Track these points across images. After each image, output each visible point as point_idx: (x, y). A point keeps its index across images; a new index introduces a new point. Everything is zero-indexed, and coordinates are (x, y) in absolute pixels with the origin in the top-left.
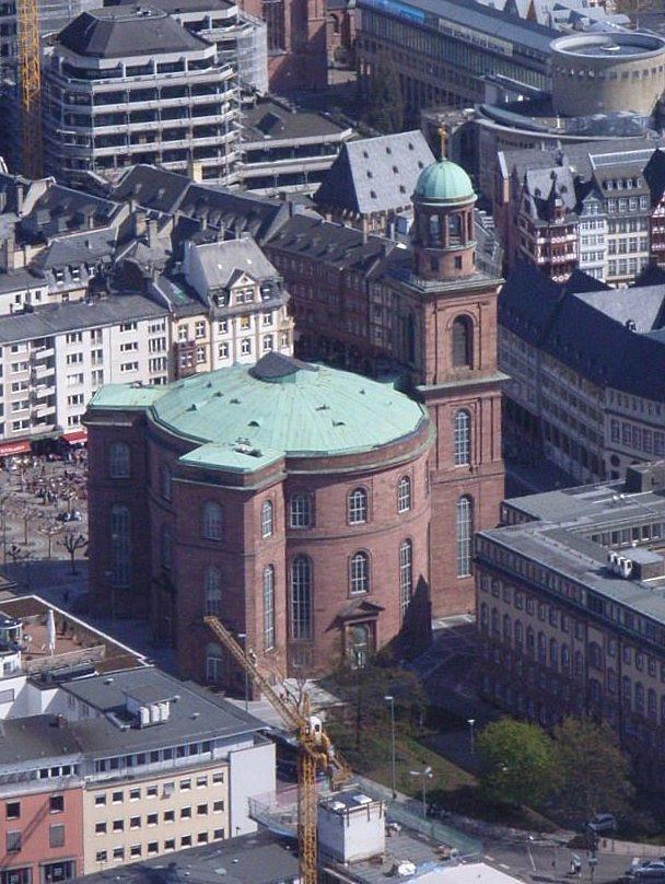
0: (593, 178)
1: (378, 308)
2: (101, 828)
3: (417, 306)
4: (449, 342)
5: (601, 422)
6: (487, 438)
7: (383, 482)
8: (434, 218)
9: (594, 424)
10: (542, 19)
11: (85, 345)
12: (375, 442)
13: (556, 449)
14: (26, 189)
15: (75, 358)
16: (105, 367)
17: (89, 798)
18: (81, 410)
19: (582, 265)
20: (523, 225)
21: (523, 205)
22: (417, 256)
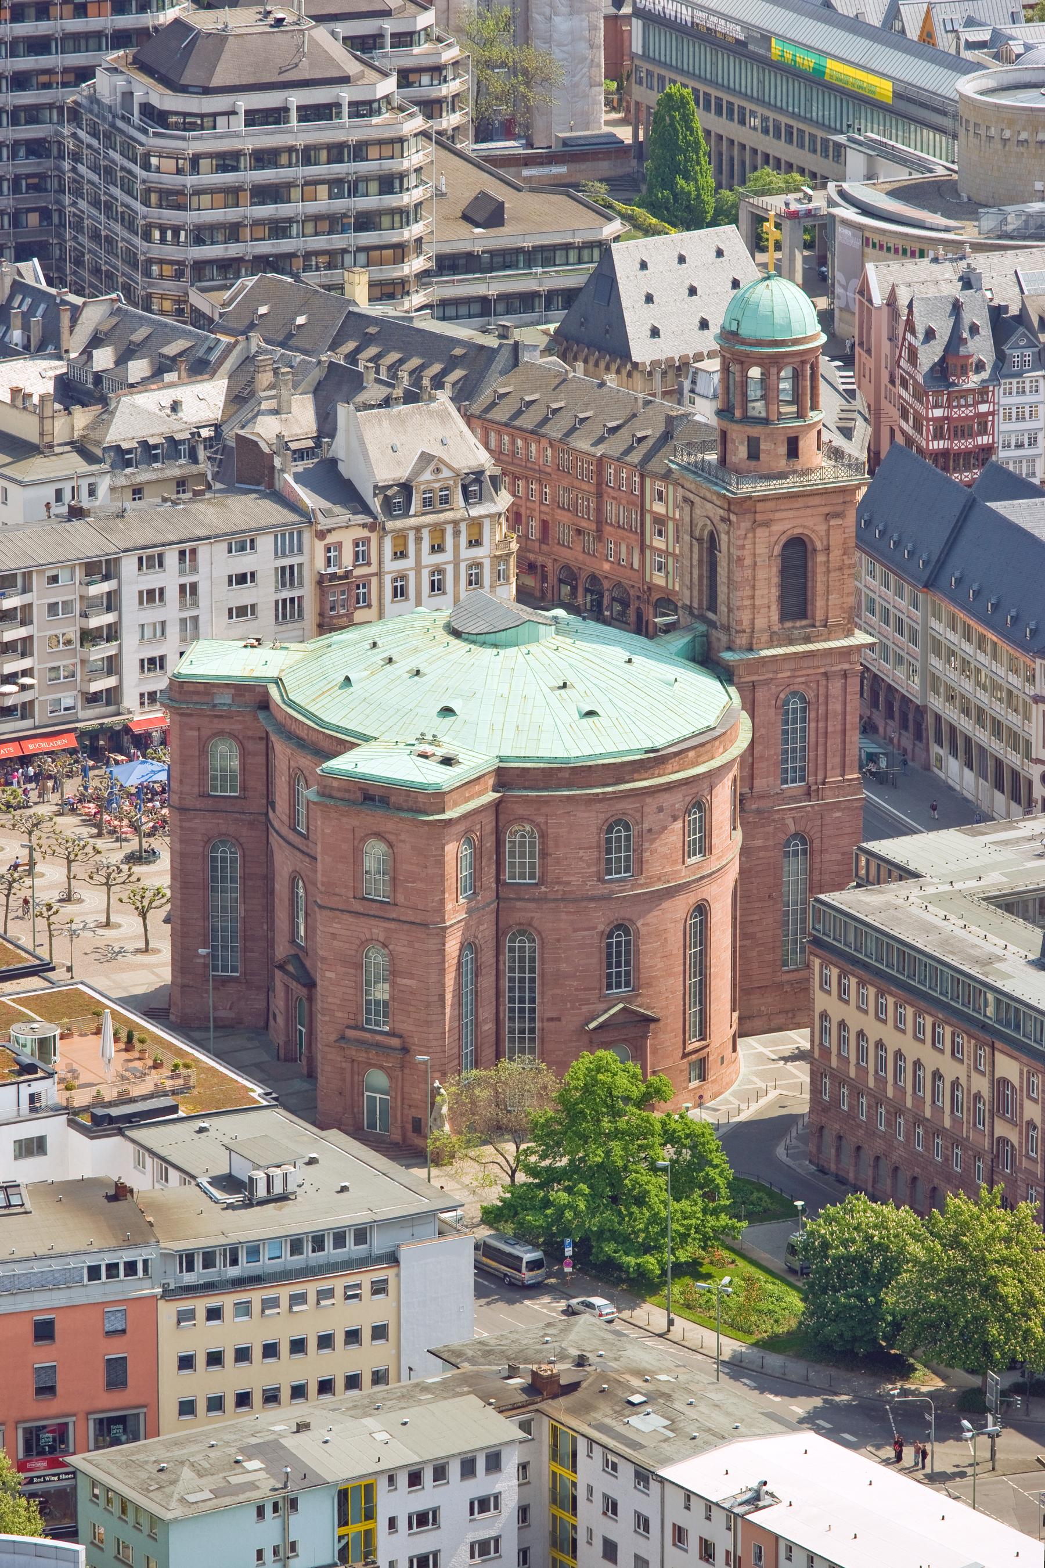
0: (1024, 309)
1: (660, 521)
2: (186, 1362)
3: (723, 519)
4: (775, 580)
5: (1027, 717)
6: (835, 742)
7: (660, 809)
8: (755, 372)
9: (1014, 720)
10: (945, 42)
11: (169, 578)
12: (648, 745)
13: (952, 760)
14: (76, 312)
15: (152, 596)
16: (203, 611)
17: (167, 1311)
18: (159, 683)
19: (1002, 455)
20: (904, 384)
21: (905, 354)
22: (724, 434)
